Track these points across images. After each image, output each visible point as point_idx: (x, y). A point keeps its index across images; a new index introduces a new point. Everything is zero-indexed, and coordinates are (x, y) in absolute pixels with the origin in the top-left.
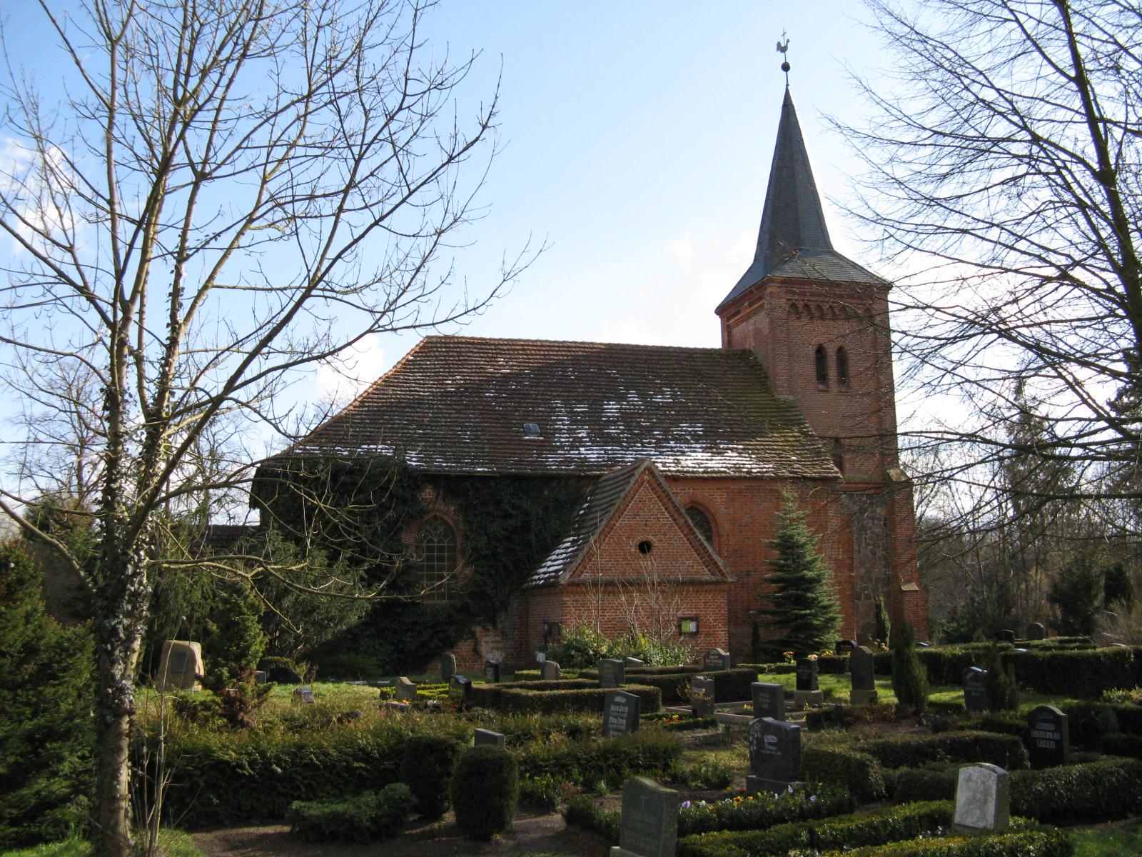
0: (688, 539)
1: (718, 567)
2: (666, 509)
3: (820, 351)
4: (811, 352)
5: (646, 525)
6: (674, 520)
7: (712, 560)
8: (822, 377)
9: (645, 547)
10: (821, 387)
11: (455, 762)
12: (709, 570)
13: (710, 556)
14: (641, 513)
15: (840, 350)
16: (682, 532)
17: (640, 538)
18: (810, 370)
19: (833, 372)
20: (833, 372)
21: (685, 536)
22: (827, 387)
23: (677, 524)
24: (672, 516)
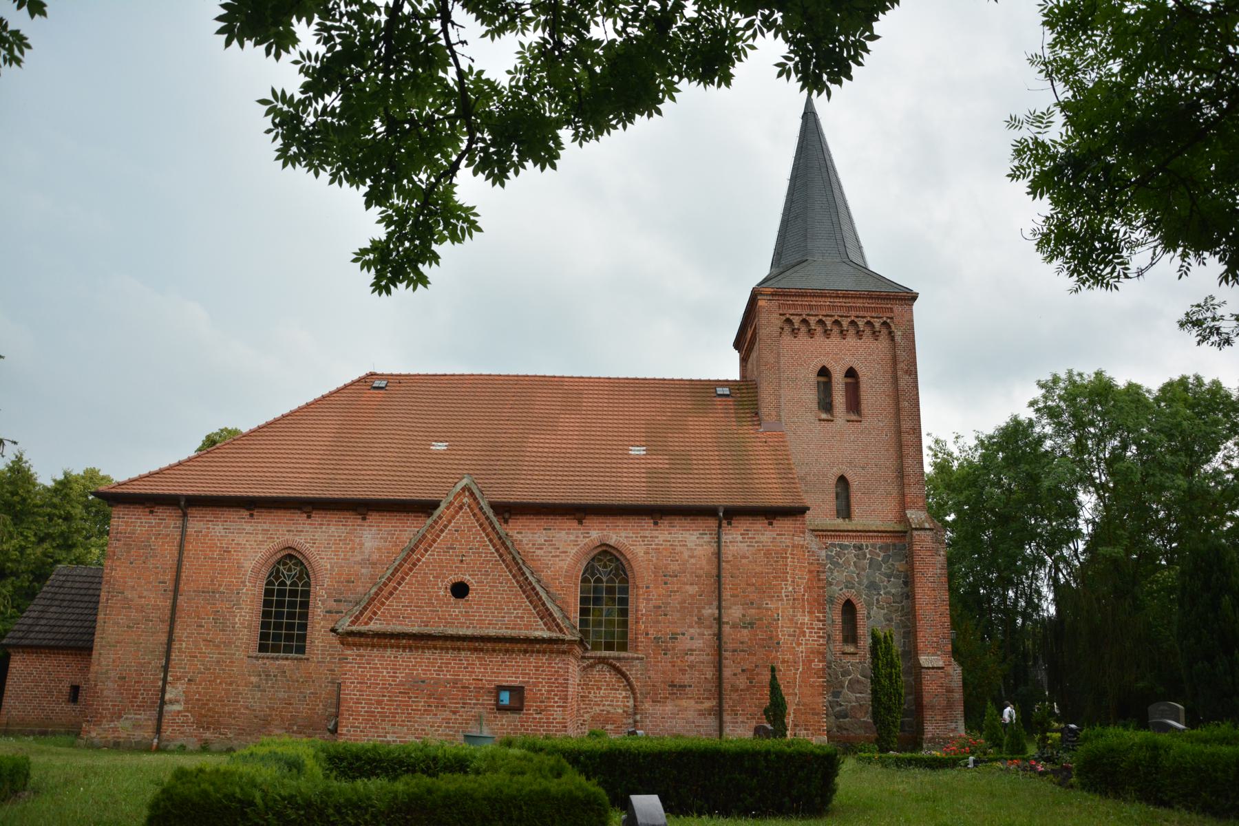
0: (518, 582)
1: (554, 620)
2: (491, 541)
3: (824, 372)
4: (813, 377)
5: (462, 561)
6: (501, 556)
7: (547, 609)
8: (826, 405)
9: (460, 590)
10: (824, 416)
11: (256, 820)
12: (545, 624)
13: (544, 604)
14: (457, 545)
15: (851, 373)
16: (510, 571)
17: (454, 578)
18: (810, 396)
19: (839, 398)
20: (839, 398)
21: (514, 576)
22: (832, 415)
23: (504, 561)
24: (497, 550)
